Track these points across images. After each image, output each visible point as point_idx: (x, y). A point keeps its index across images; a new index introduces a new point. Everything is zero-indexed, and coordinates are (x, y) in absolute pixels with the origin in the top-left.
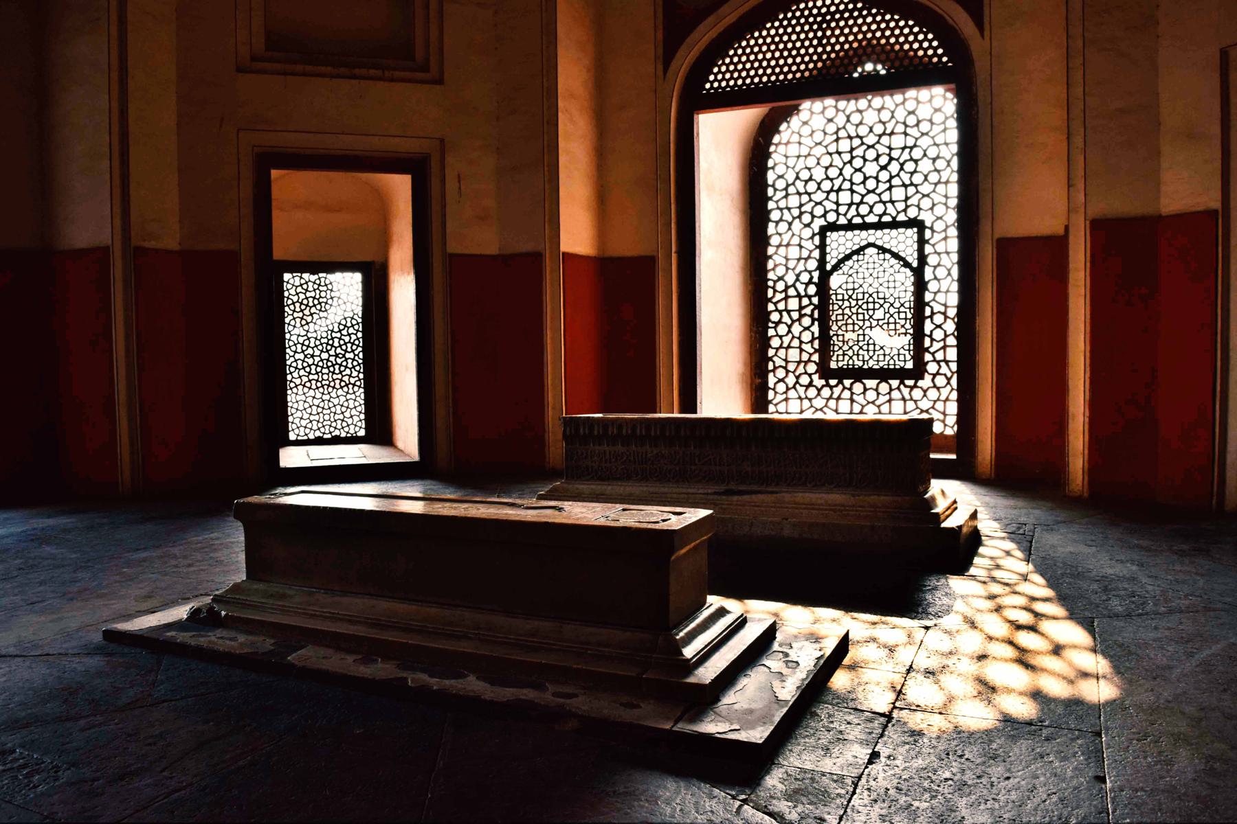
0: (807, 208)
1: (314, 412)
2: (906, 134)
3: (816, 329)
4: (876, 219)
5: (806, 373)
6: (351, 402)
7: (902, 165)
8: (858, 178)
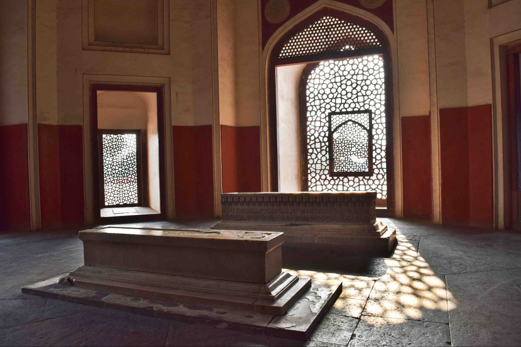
0: (323, 105)
1: (116, 193)
2: (363, 74)
3: (327, 156)
4: (351, 110)
5: (324, 174)
6: (132, 189)
7: (362, 87)
8: (344, 93)
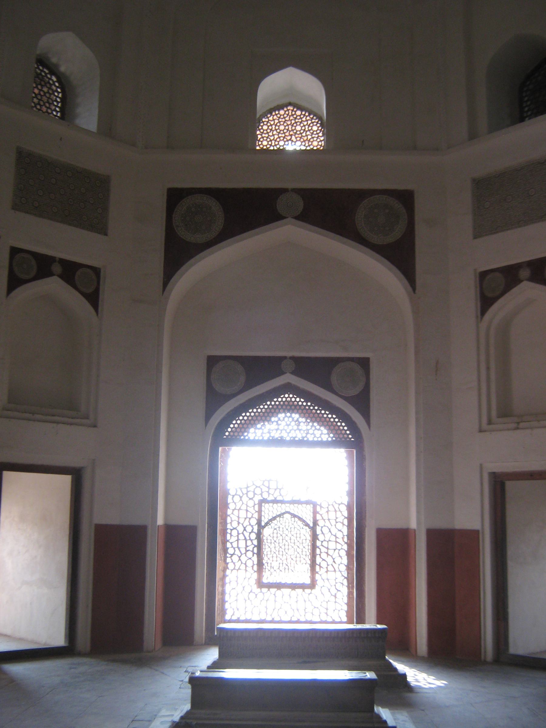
3: (255, 558)
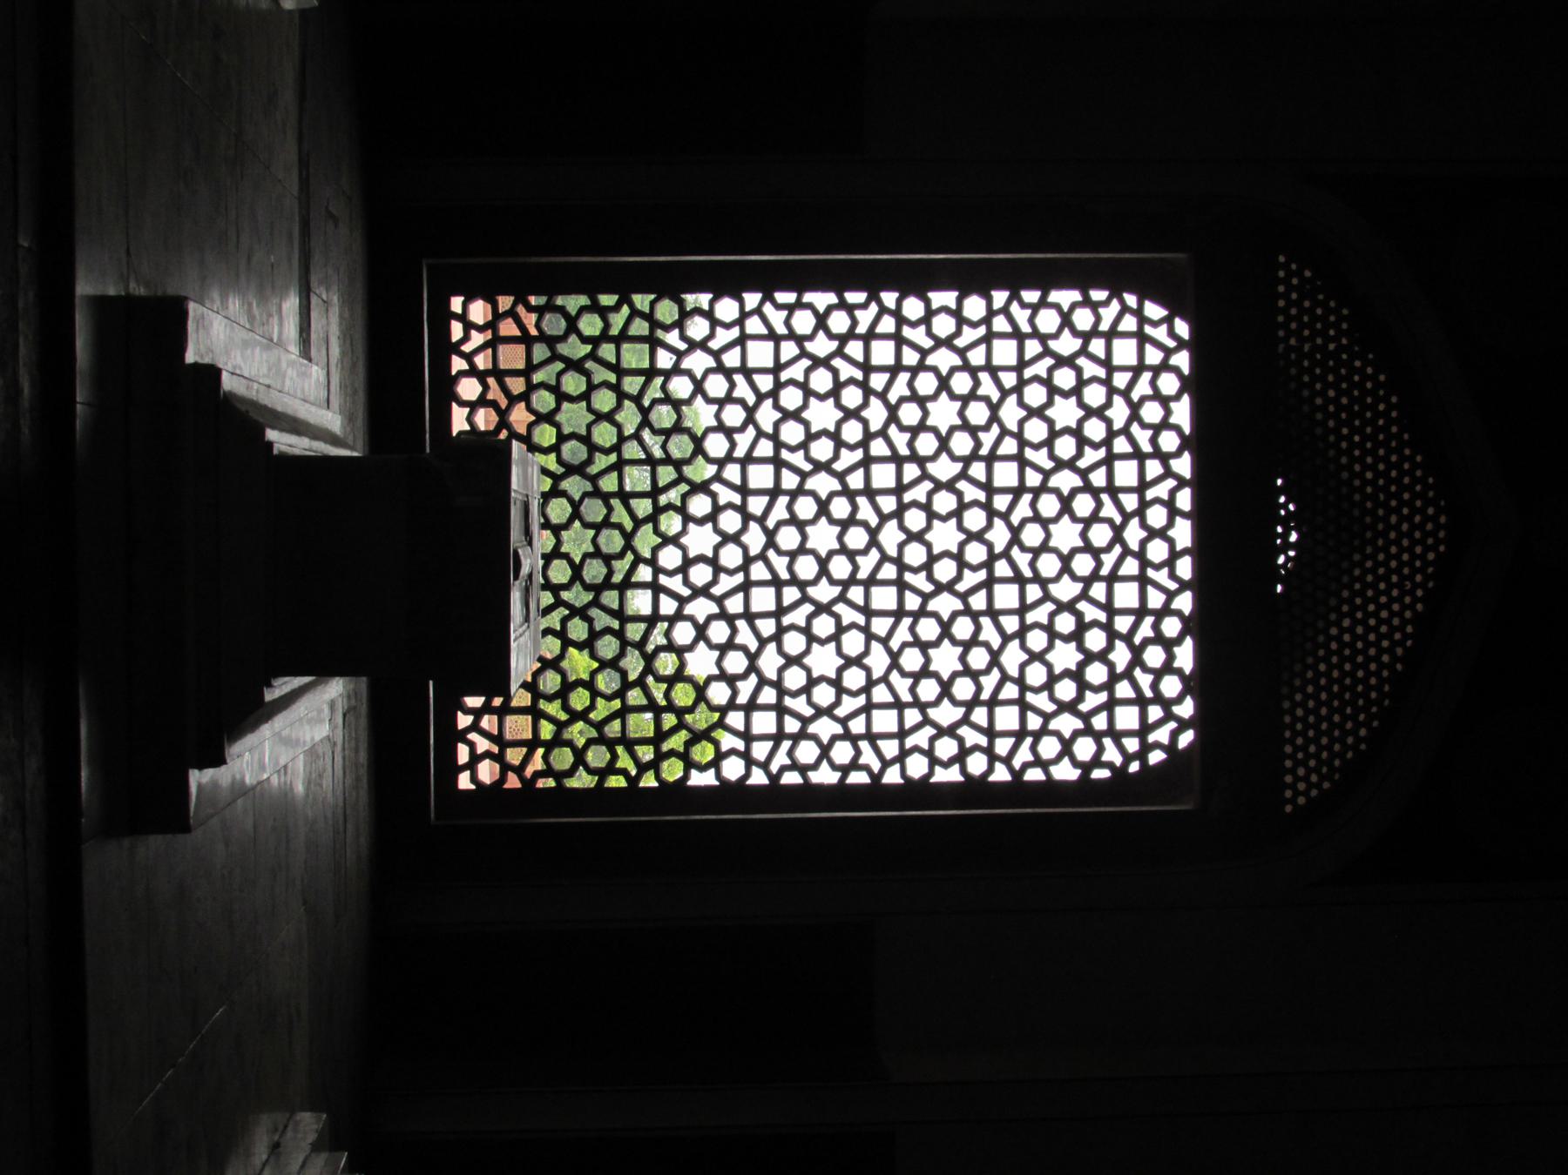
5: (592, 387)
